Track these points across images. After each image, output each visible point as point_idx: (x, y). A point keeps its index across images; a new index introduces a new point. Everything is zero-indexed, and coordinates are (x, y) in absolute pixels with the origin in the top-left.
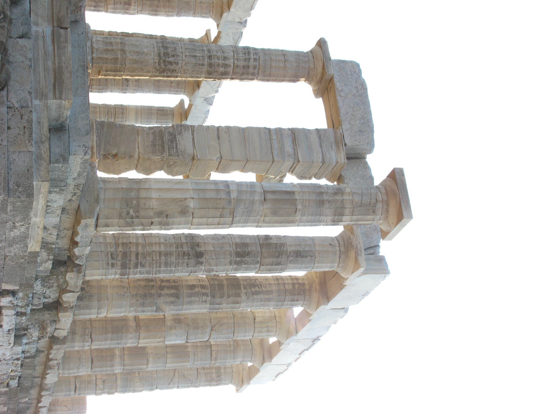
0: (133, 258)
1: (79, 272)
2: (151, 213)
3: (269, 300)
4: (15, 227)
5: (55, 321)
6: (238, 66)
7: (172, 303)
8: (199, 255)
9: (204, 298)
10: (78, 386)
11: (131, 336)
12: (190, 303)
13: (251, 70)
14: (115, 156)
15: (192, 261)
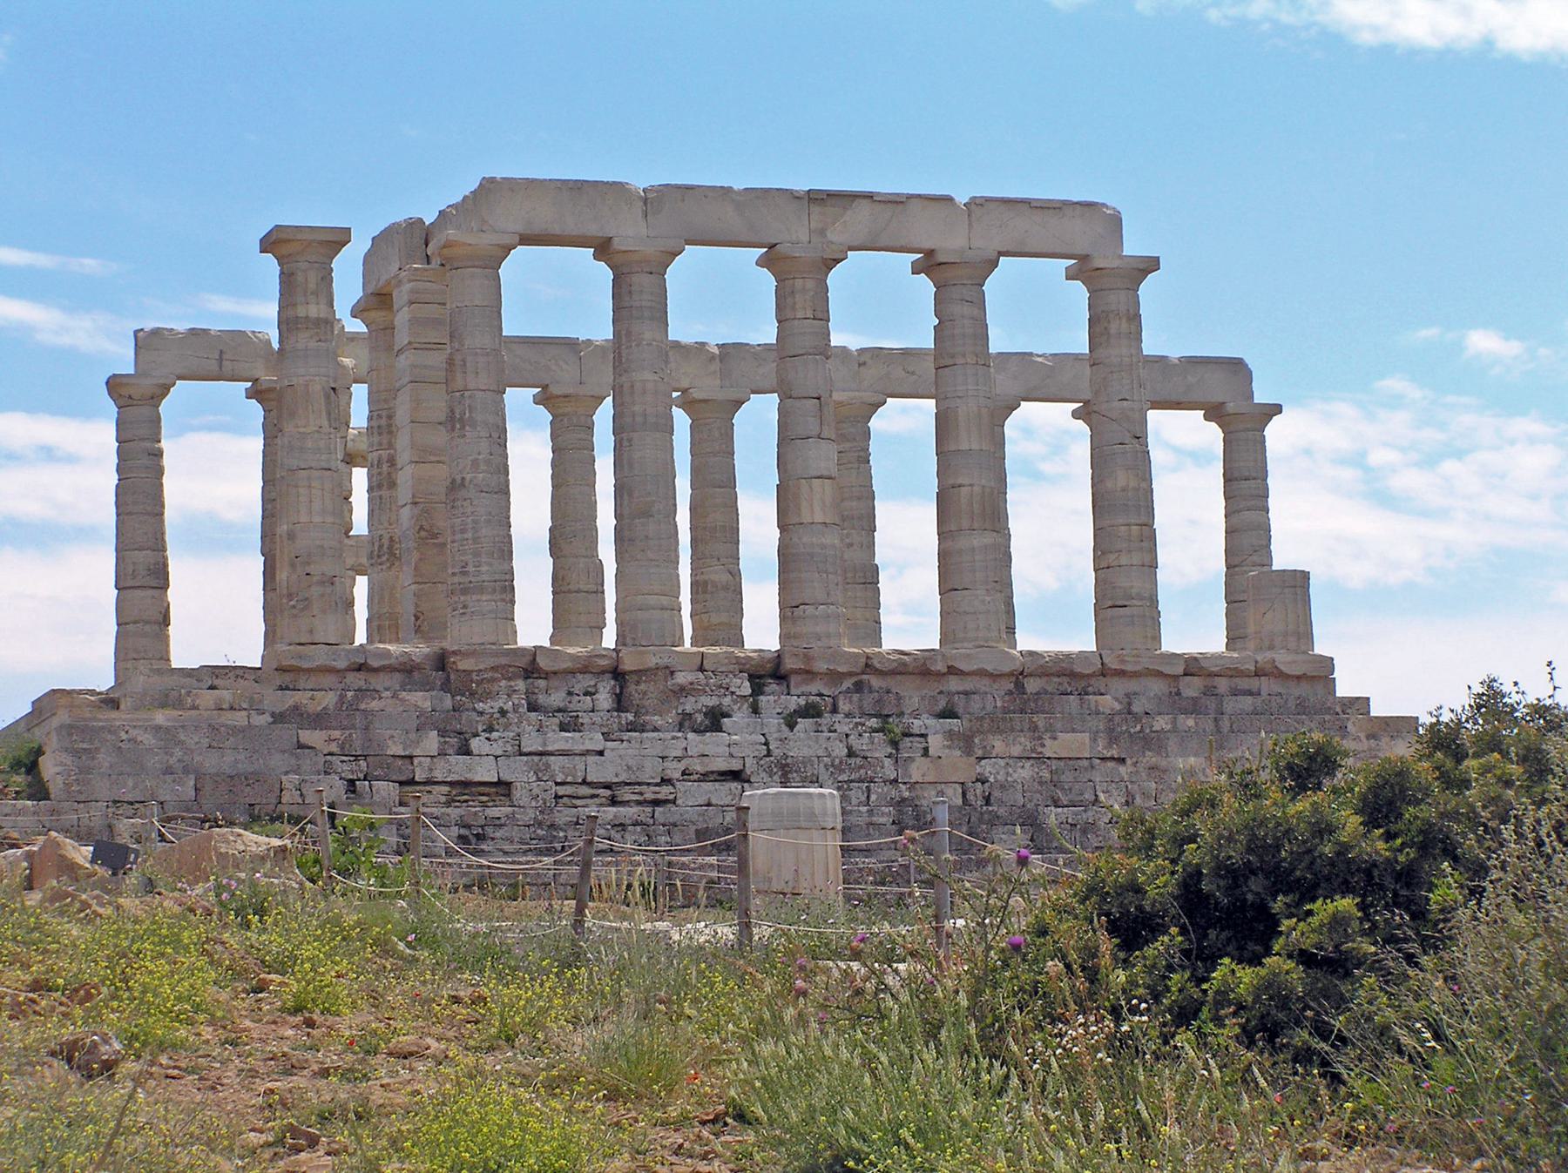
0: (456, 579)
1: (454, 653)
2: (294, 577)
3: (629, 333)
4: (133, 740)
5: (672, 673)
6: (380, 444)
7: (630, 495)
8: (454, 481)
9: (625, 443)
10: (1110, 603)
11: (795, 539)
12: (631, 466)
13: (383, 422)
14: (417, 618)
15: (463, 493)
